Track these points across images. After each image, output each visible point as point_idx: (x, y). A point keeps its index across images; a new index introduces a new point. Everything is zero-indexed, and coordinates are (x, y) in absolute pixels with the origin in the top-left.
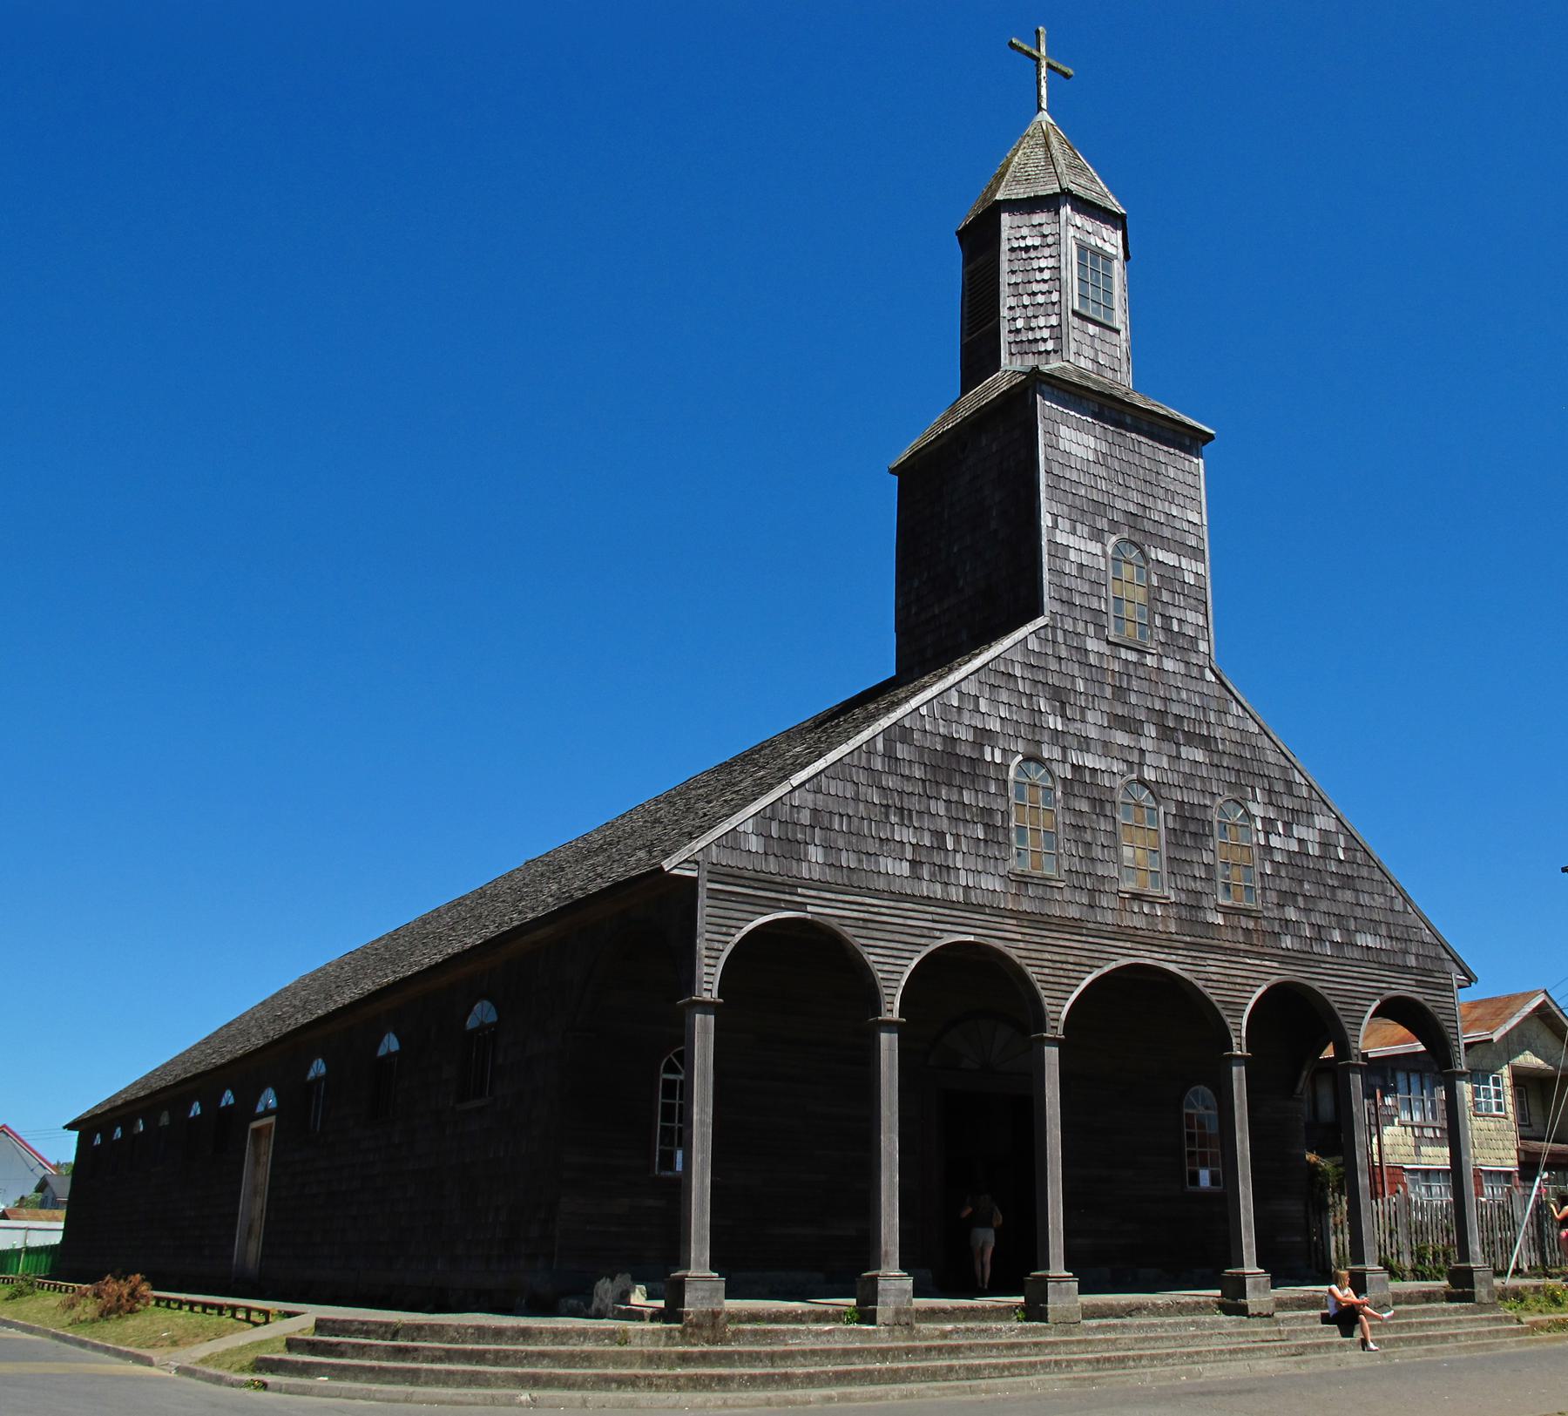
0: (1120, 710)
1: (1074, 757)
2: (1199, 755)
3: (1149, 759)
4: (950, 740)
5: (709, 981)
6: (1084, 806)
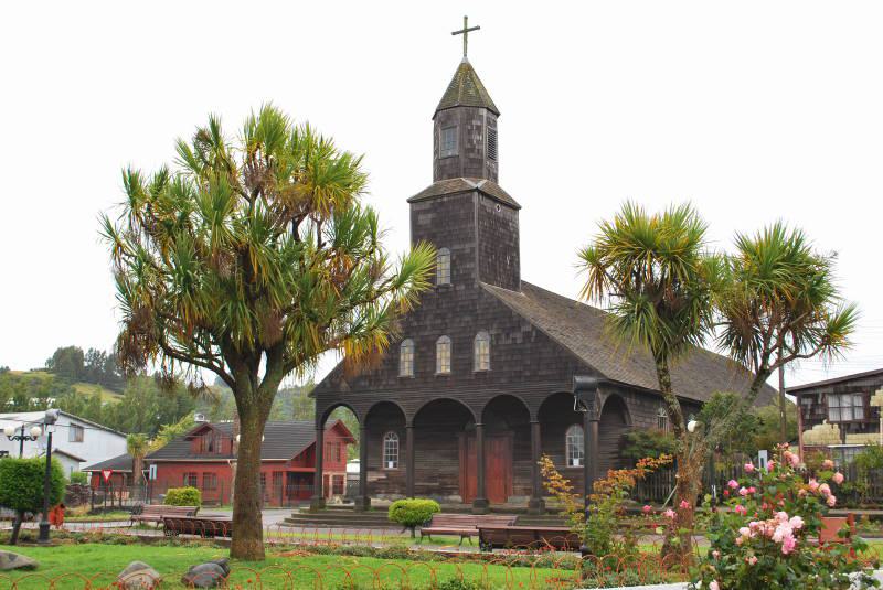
0: (439, 312)
2: (467, 318)
6: (423, 349)
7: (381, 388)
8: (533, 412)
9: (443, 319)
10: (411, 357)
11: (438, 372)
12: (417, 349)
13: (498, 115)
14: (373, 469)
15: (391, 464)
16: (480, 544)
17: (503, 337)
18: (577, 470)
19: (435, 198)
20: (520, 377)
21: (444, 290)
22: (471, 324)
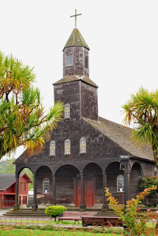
0: (65, 129)
1: (58, 138)
2: (77, 132)
3: (70, 135)
6: (59, 144)
7: (42, 160)
8: (104, 169)
9: (67, 132)
10: (54, 148)
11: (65, 153)
12: (57, 144)
13: (89, 50)
14: (39, 193)
15: (46, 191)
16: (83, 224)
17: (92, 139)
18: (121, 193)
19: (63, 83)
20: (98, 155)
22: (79, 134)
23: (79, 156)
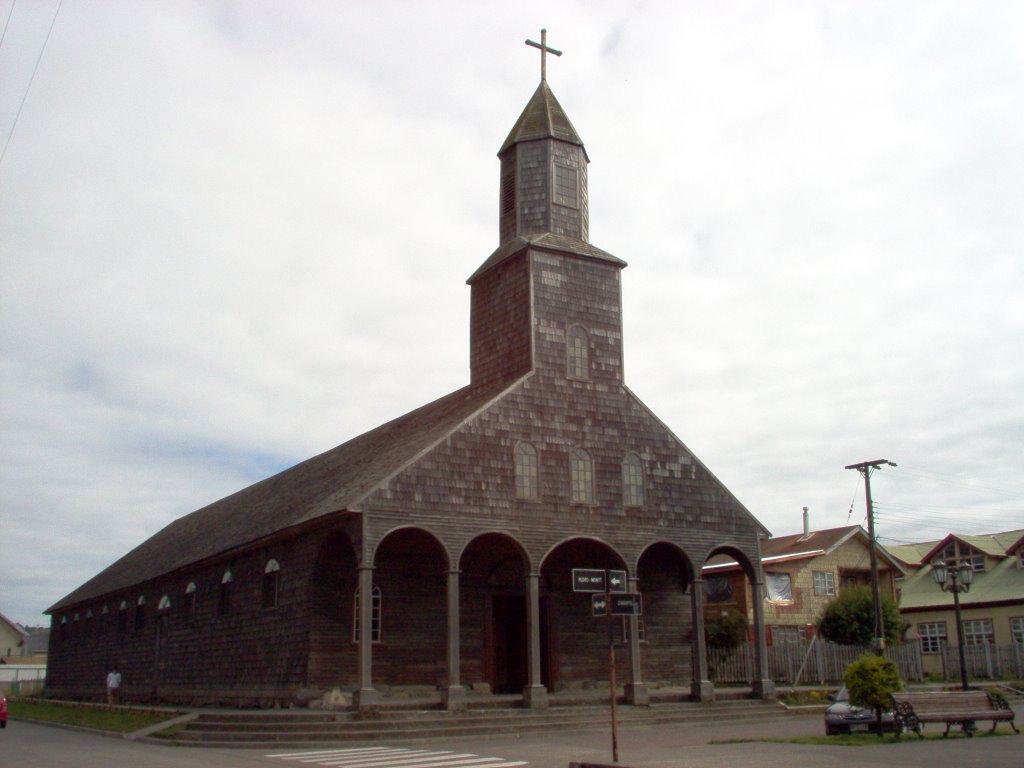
2: (611, 432)
3: (588, 437)
4: (484, 436)
5: (368, 558)
21: (579, 386)
23: (624, 514)
